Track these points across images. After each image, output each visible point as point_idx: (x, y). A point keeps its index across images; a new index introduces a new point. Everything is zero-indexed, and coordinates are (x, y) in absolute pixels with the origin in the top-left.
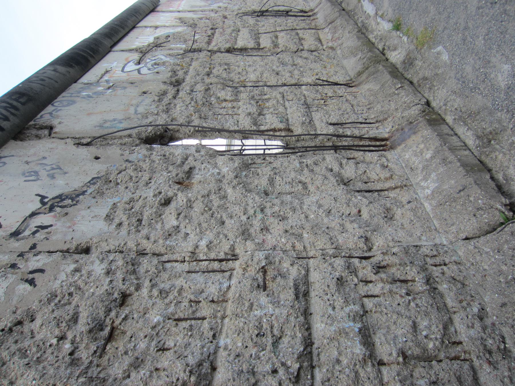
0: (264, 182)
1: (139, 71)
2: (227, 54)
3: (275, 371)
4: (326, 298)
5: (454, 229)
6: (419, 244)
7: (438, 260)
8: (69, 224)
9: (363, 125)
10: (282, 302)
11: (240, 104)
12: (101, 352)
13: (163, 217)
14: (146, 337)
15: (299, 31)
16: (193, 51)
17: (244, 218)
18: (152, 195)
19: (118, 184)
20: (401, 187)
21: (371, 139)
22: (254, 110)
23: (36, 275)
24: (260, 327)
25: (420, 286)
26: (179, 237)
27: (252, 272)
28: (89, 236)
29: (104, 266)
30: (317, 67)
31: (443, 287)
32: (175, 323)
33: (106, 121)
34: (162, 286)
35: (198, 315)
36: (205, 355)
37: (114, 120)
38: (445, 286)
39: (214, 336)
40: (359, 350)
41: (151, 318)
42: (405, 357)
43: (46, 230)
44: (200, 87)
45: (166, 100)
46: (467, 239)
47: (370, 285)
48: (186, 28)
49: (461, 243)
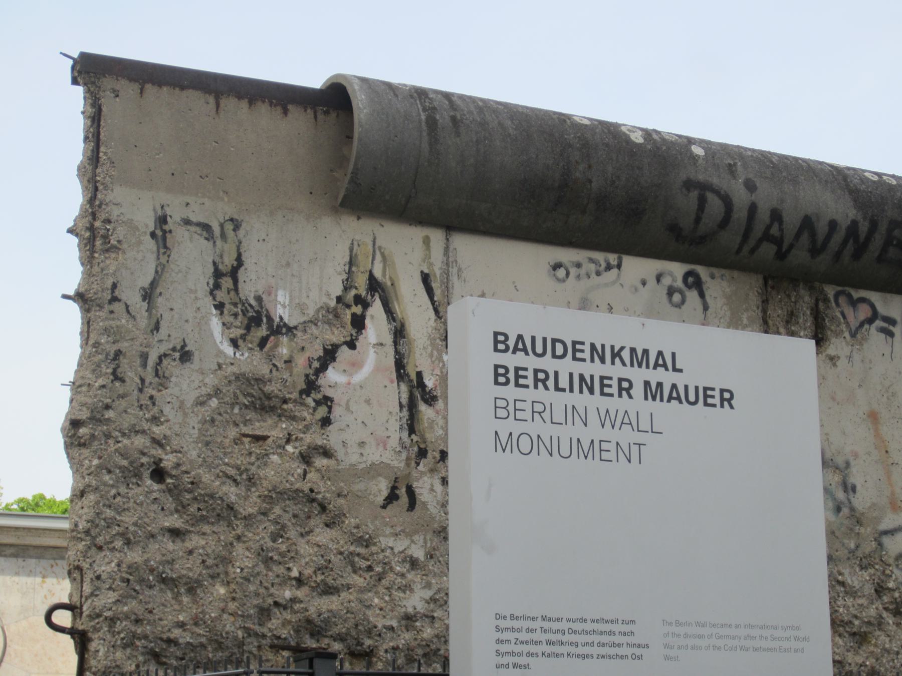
23: (404, 499)
29: (421, 607)
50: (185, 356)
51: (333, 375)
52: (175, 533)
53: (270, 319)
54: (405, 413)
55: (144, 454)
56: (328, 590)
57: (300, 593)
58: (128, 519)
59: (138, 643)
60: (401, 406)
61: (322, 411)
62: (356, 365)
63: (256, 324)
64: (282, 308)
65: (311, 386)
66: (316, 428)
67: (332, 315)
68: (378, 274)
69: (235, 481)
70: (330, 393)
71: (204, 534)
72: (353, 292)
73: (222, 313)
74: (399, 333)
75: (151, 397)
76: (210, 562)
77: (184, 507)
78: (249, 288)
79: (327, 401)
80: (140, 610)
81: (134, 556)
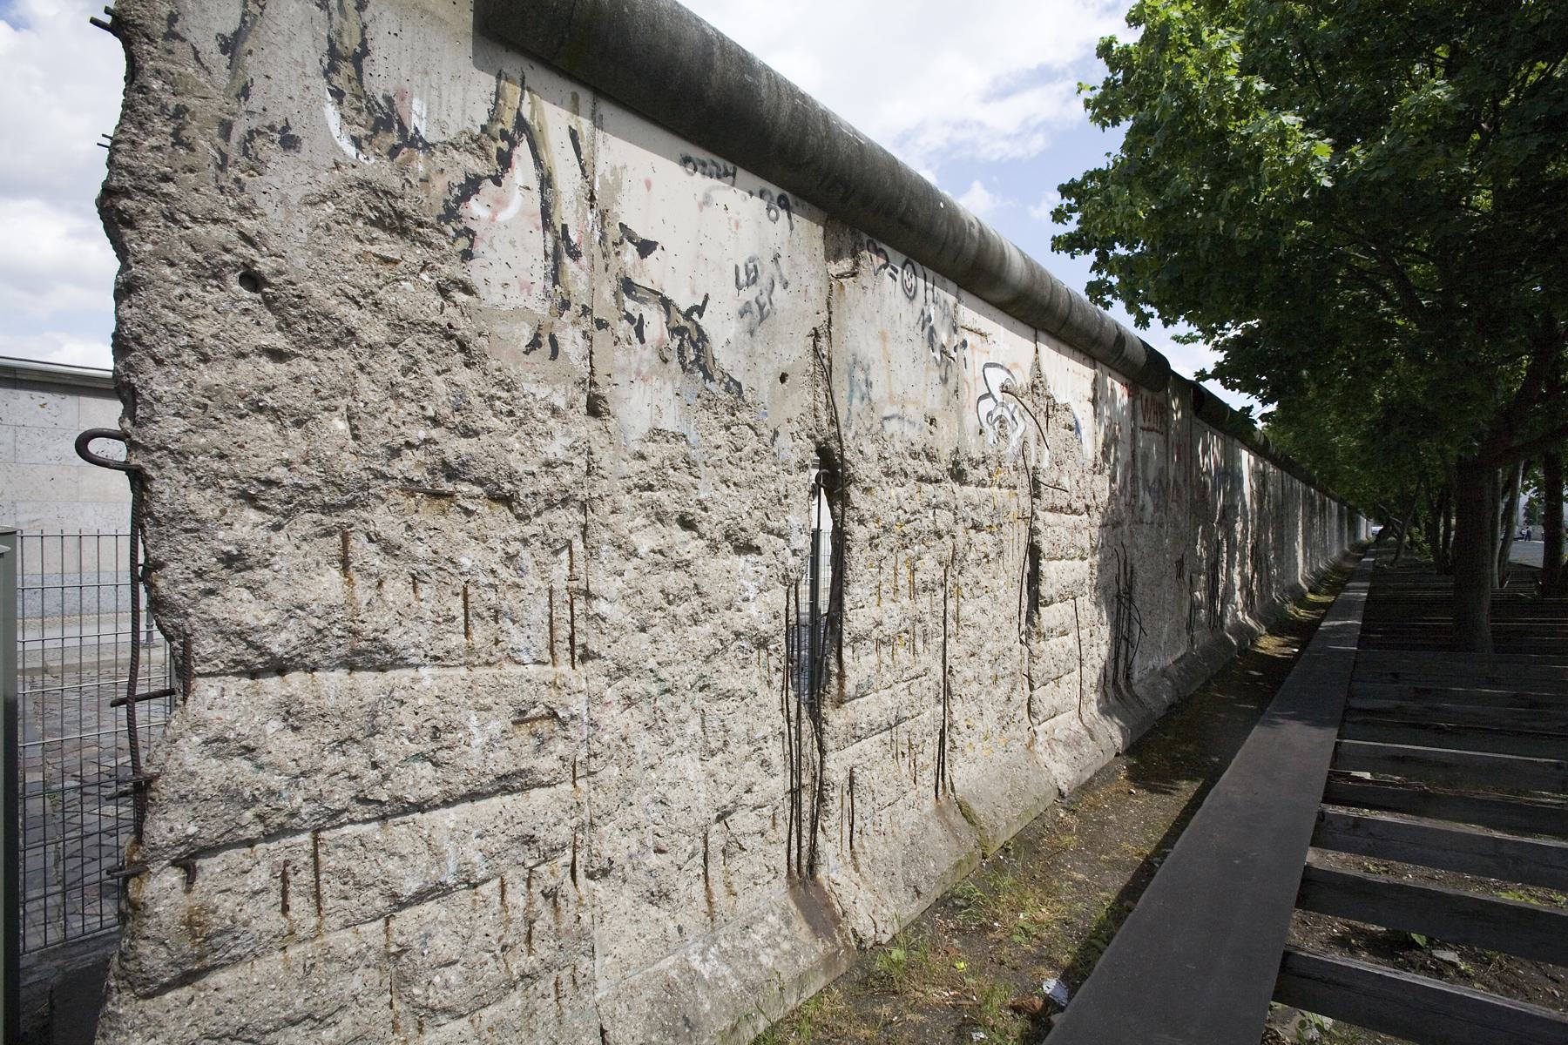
0: (725, 683)
1: (989, 394)
2: (1023, 547)
3: (375, 766)
4: (500, 822)
5: (622, 1009)
6: (597, 955)
7: (567, 986)
8: (644, 370)
9: (847, 828)
10: (491, 755)
11: (906, 601)
12: (410, 487)
13: (659, 525)
14: (435, 552)
15: (1076, 674)
16: (1035, 484)
17: (652, 663)
18: (702, 496)
19: (728, 428)
20: (711, 915)
21: (813, 848)
22: (889, 628)
23: (547, 348)
24: (450, 728)
25: (520, 963)
26: (616, 563)
27: (548, 695)
28: (619, 412)
29: (562, 455)
30: (990, 721)
31: (516, 999)
32: (460, 590)
33: (866, 370)
34: (525, 554)
35: (476, 622)
36: (404, 654)
37: (869, 384)
38: (519, 1002)
39: (436, 658)
40: (410, 886)
41: (466, 552)
42: (398, 955)
43: (633, 336)
44: (944, 519)
45: (910, 464)
46: (603, 1032)
47: (523, 886)
48: (1091, 457)
49: (595, 1025)
50: (289, 142)
51: (476, 208)
52: (277, 355)
53: (403, 129)
54: (550, 262)
55: (228, 251)
56: (468, 433)
57: (435, 433)
58: (203, 328)
59: (223, 483)
60: (546, 255)
61: (463, 243)
62: (501, 203)
63: (383, 123)
64: (418, 117)
65: (450, 214)
66: (456, 259)
67: (476, 144)
68: (526, 113)
69: (357, 303)
70: (473, 226)
71: (316, 359)
72: (500, 126)
73: (340, 103)
74: (546, 182)
75: (237, 180)
76: (324, 392)
77: (288, 325)
78: (379, 82)
79: (469, 233)
80: (226, 444)
81: (210, 376)
